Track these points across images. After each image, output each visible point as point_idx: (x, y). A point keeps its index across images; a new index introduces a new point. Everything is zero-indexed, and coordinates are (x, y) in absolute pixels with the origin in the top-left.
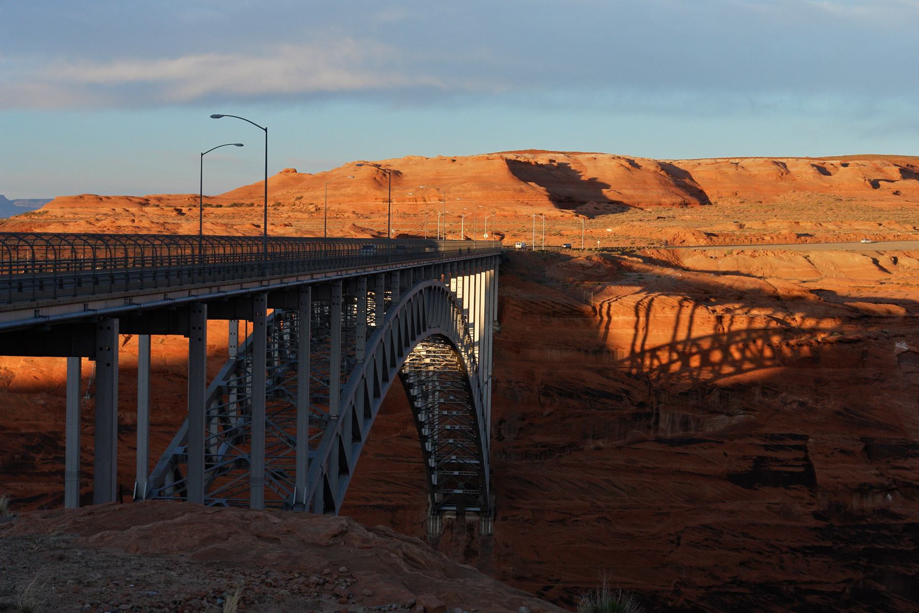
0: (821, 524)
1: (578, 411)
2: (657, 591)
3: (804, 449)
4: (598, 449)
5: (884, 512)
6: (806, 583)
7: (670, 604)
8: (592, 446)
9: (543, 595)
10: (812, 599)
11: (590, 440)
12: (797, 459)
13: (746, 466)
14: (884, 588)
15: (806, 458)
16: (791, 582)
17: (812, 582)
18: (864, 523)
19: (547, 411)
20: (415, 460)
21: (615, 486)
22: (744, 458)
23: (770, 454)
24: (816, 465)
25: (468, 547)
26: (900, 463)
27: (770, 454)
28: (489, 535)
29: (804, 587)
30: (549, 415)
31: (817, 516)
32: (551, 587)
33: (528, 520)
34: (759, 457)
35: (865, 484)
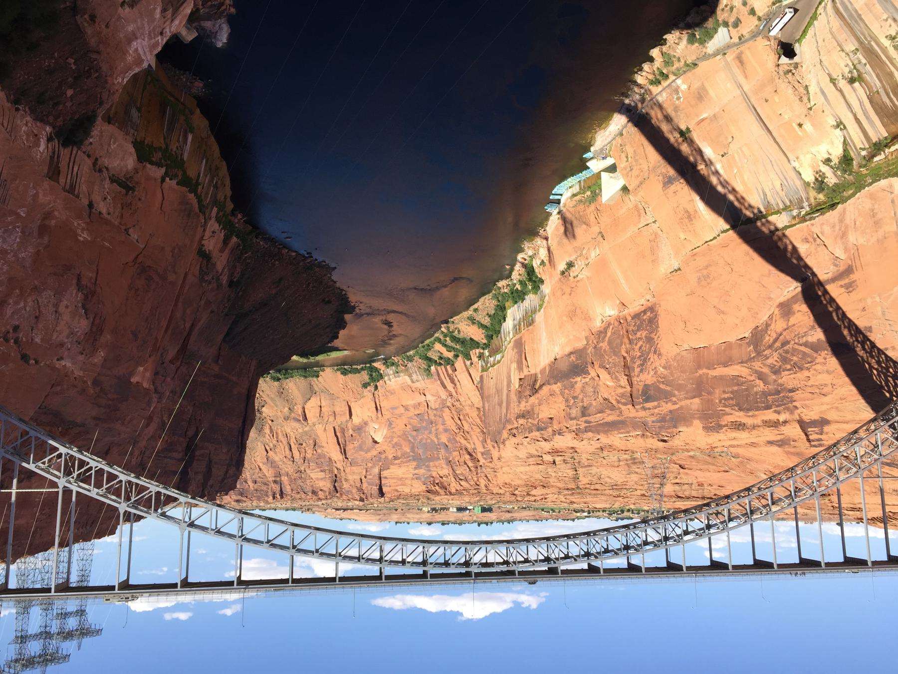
0: (794, 404)
3: (809, 440)
5: (779, 413)
6: (792, 374)
7: (826, 352)
10: (789, 367)
12: (811, 435)
13: (826, 429)
14: (774, 377)
15: (806, 435)
16: (795, 373)
17: (790, 375)
18: (783, 407)
22: (827, 433)
23: (820, 437)
24: (803, 434)
26: (781, 437)
27: (820, 437)
29: (792, 372)
31: (796, 407)
34: (822, 434)
35: (785, 426)
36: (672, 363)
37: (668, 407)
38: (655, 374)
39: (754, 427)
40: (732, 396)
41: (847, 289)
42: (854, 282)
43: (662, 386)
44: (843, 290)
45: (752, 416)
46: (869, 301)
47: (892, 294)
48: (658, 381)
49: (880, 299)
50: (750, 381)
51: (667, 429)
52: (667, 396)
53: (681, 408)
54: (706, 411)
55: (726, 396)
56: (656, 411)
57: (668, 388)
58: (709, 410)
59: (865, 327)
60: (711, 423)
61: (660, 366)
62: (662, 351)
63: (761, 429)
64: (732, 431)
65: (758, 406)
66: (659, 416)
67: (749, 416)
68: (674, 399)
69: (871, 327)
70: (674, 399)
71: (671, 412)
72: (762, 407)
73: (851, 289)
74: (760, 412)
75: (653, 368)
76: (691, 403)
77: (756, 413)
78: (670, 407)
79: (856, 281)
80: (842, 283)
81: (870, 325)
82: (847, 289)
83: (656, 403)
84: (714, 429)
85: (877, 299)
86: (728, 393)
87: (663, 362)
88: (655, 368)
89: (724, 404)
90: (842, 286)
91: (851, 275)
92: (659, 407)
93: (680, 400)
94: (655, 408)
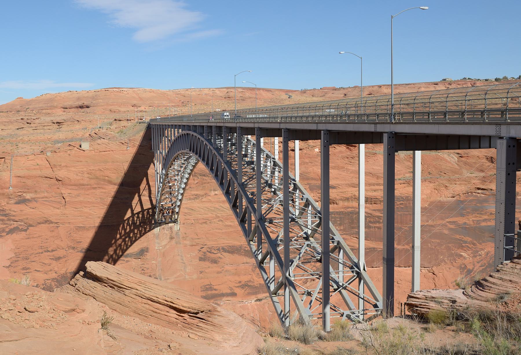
1: (207, 181)
2: (242, 245)
4: (216, 195)
8: (213, 194)
9: (201, 250)
11: (212, 192)
19: (196, 182)
20: (147, 204)
21: (224, 208)
25: (170, 235)
28: (178, 230)
30: (197, 183)
32: (203, 247)
33: (192, 223)
36: (446, 259)
37: (461, 220)
38: (477, 252)
39: (347, 199)
40: (370, 224)
41: (211, 287)
42: (204, 291)
43: (469, 239)
44: (215, 287)
45: (348, 208)
46: (195, 276)
47: (175, 278)
48: (474, 244)
49: (185, 276)
50: (347, 234)
51: (473, 200)
52: (466, 229)
53: (442, 219)
54: (406, 215)
55: (377, 225)
56: (486, 217)
57: (458, 237)
58: (401, 215)
59: (205, 261)
60: (401, 204)
61: (465, 258)
62: (458, 271)
63: (338, 197)
64: (375, 196)
65: (340, 215)
66: (482, 213)
67: (351, 208)
68: (452, 226)
69: (200, 260)
70: (452, 226)
71: (462, 215)
72: (334, 214)
73: (207, 287)
74: (337, 211)
75: (478, 257)
76: (428, 221)
77: (342, 210)
78: (461, 220)
79: (201, 291)
80: (214, 292)
81: (201, 262)
82: (211, 287)
83: (483, 224)
84: (398, 199)
85: (187, 277)
86: (375, 227)
87: (459, 261)
88: (476, 256)
89: (380, 219)
90: (216, 290)
91: (205, 295)
92: (478, 221)
93: (443, 225)
94: (485, 220)
